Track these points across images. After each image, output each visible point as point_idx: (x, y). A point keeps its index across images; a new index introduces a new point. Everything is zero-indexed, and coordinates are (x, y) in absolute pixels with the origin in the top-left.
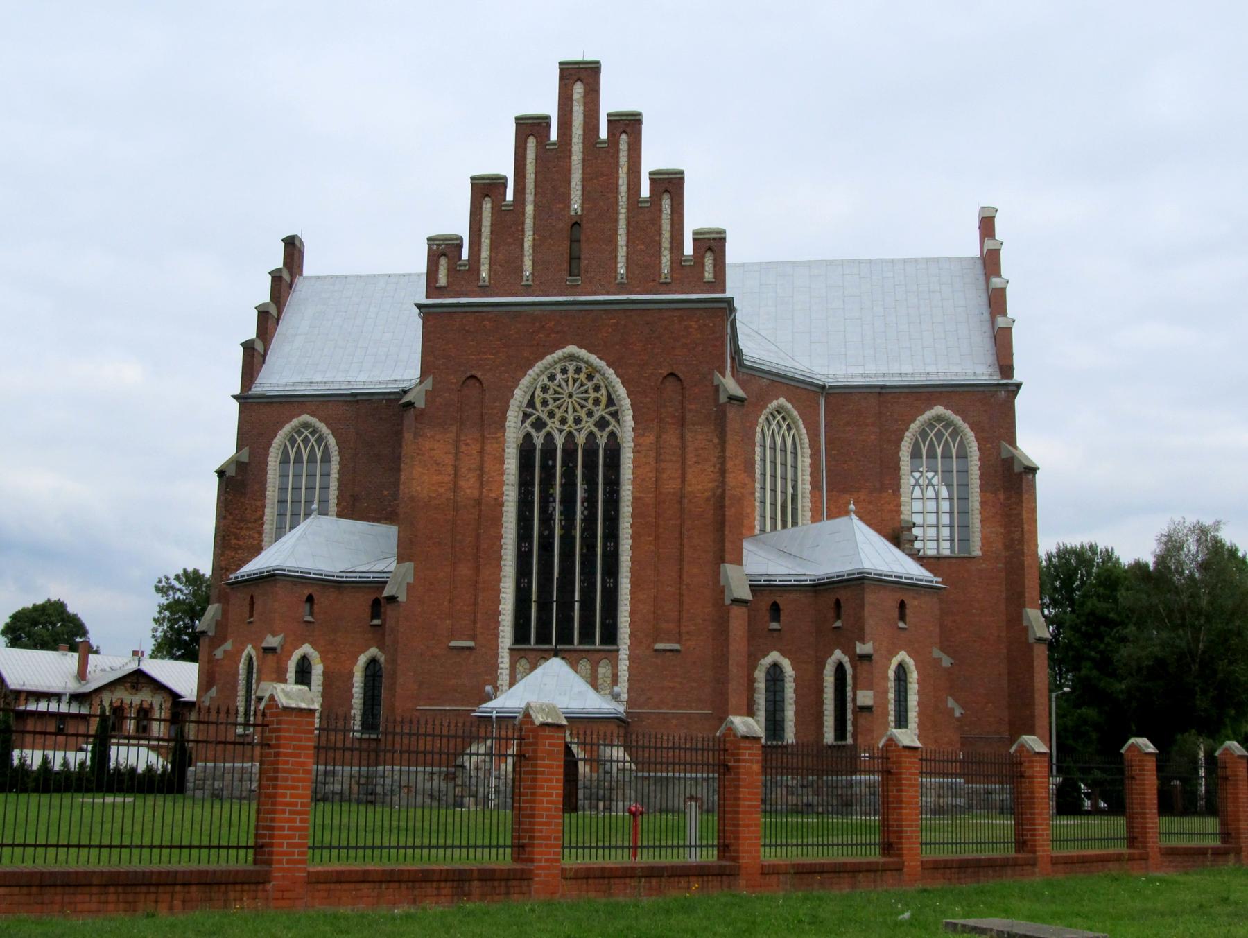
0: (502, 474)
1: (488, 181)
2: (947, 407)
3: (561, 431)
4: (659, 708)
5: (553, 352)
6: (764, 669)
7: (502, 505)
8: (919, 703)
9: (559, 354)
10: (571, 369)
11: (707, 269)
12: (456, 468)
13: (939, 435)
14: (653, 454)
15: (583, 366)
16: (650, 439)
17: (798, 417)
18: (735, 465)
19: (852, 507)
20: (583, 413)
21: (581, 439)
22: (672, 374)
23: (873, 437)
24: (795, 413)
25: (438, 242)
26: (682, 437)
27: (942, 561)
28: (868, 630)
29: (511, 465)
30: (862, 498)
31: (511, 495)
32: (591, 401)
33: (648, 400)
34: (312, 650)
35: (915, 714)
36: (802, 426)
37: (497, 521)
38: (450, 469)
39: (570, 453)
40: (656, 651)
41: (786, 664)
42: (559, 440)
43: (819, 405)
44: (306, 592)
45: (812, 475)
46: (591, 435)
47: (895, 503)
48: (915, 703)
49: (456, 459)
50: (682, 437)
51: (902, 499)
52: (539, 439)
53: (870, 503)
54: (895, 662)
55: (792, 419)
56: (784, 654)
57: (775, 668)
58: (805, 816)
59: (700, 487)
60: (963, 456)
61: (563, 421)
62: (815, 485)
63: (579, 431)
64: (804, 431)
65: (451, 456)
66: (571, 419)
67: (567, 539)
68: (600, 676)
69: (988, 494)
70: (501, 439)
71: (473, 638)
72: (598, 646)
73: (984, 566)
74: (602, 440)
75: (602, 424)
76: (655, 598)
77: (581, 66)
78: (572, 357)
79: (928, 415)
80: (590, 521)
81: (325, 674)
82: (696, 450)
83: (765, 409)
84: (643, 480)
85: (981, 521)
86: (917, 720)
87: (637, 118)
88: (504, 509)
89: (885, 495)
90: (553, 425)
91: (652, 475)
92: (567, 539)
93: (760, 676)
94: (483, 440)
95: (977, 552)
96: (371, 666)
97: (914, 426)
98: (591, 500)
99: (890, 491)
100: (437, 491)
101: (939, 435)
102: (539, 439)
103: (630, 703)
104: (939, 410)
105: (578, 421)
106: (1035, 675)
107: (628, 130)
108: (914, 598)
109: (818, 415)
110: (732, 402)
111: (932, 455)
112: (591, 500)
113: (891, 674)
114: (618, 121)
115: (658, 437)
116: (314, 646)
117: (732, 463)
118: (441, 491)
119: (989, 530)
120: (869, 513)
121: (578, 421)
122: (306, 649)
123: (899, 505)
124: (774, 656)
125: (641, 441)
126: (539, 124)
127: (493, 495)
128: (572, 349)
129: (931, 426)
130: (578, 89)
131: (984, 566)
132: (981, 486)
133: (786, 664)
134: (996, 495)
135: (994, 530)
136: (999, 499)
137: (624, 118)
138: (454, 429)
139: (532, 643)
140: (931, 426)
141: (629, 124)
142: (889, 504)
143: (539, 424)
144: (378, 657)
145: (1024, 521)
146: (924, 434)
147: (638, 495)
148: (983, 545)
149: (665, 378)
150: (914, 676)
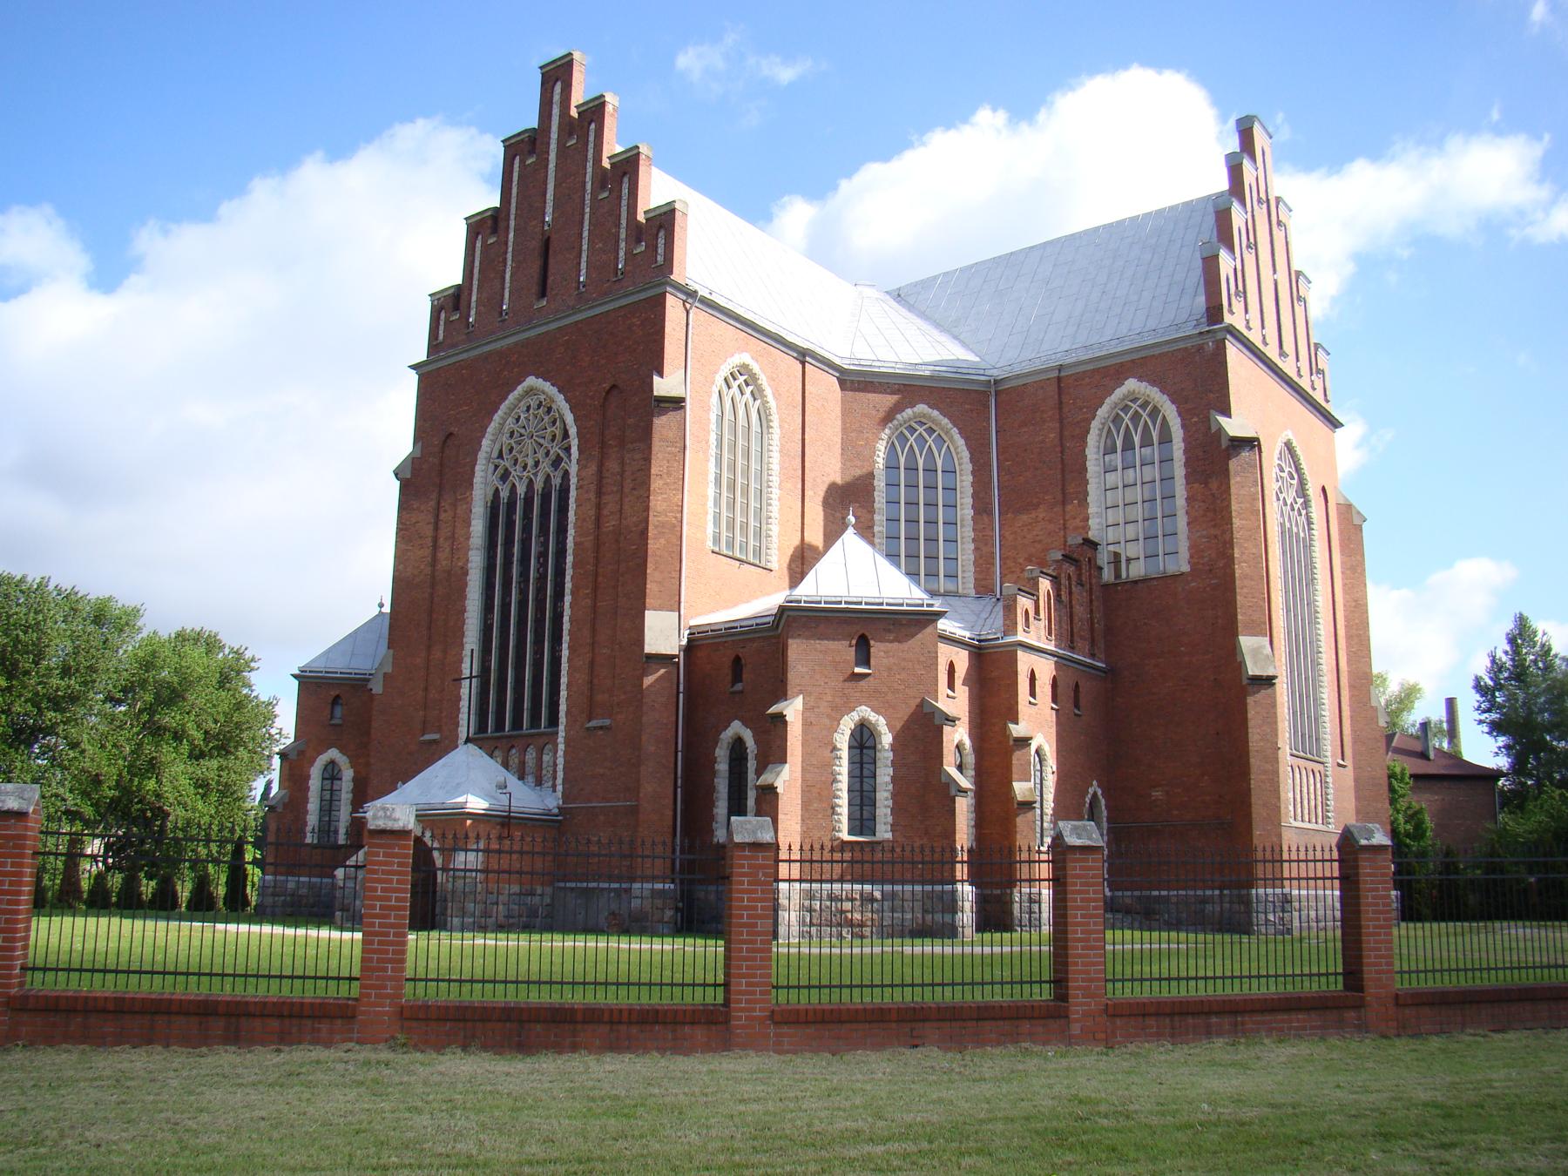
0: (468, 538)
1: (479, 218)
2: (1140, 379)
3: (521, 478)
4: (590, 801)
5: (515, 389)
6: (725, 745)
7: (466, 574)
8: (894, 779)
9: (520, 388)
10: (534, 404)
11: (659, 251)
12: (435, 539)
13: (1136, 417)
14: (593, 487)
15: (542, 397)
16: (593, 468)
17: (950, 426)
18: (667, 484)
19: (852, 519)
20: (541, 453)
21: (539, 485)
22: (614, 387)
23: (1052, 435)
24: (945, 421)
25: (438, 297)
26: (623, 464)
27: (1140, 585)
28: (792, 676)
29: (478, 527)
30: (1041, 516)
31: (476, 562)
32: (549, 437)
33: (592, 423)
34: (340, 755)
35: (887, 794)
36: (957, 437)
37: (462, 595)
38: (429, 541)
39: (528, 501)
40: (588, 729)
41: (748, 736)
42: (521, 490)
43: (988, 407)
44: (333, 693)
45: (975, 496)
46: (548, 478)
47: (1081, 517)
48: (888, 779)
49: (436, 529)
50: (623, 464)
51: (1090, 511)
52: (504, 494)
53: (1050, 521)
54: (847, 724)
55: (942, 429)
56: (745, 723)
57: (738, 743)
58: (867, 941)
59: (635, 519)
60: (1166, 439)
61: (525, 467)
62: (981, 508)
63: (535, 475)
64: (961, 442)
65: (431, 527)
66: (530, 462)
67: (523, 604)
68: (544, 765)
69: (1196, 485)
70: (469, 499)
71: (439, 730)
72: (542, 729)
73: (1193, 584)
74: (556, 481)
75: (557, 462)
76: (592, 663)
77: (559, 63)
78: (531, 391)
79: (1119, 393)
80: (542, 578)
81: (355, 780)
82: (633, 474)
83: (891, 421)
84: (584, 520)
85: (1188, 524)
86: (890, 803)
87: (602, 100)
88: (468, 578)
89: (1069, 508)
90: (515, 472)
91: (592, 512)
92: (523, 604)
93: (722, 754)
94: (454, 505)
95: (1186, 568)
96: (330, 767)
97: (1102, 412)
98: (543, 555)
99: (1075, 502)
100: (418, 567)
101: (1136, 417)
102: (504, 495)
103: (565, 797)
104: (1131, 384)
105: (537, 464)
106: (1250, 730)
107: (595, 117)
108: (889, 631)
109: (989, 419)
110: (662, 405)
111: (1128, 445)
112: (543, 555)
113: (843, 740)
114: (586, 110)
115: (601, 465)
116: (343, 750)
117: (661, 482)
118: (422, 567)
119: (1199, 534)
120: (1049, 534)
121: (537, 464)
122: (333, 753)
123: (1087, 519)
124: (736, 728)
125: (584, 474)
126: (522, 140)
127: (460, 564)
128: (531, 381)
129: (1126, 409)
130: (558, 88)
131: (1193, 584)
132: (1187, 476)
133: (748, 736)
134: (1206, 484)
135: (1205, 533)
136: (1210, 490)
137: (591, 105)
138: (434, 496)
139: (507, 729)
140: (1126, 409)
141: (595, 111)
142: (1075, 518)
143: (505, 476)
144: (337, 760)
145: (1234, 514)
146: (1117, 420)
147: (578, 539)
148: (1191, 557)
149: (608, 392)
150: (887, 739)
